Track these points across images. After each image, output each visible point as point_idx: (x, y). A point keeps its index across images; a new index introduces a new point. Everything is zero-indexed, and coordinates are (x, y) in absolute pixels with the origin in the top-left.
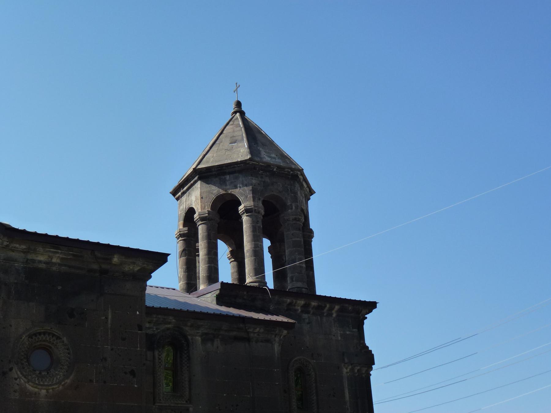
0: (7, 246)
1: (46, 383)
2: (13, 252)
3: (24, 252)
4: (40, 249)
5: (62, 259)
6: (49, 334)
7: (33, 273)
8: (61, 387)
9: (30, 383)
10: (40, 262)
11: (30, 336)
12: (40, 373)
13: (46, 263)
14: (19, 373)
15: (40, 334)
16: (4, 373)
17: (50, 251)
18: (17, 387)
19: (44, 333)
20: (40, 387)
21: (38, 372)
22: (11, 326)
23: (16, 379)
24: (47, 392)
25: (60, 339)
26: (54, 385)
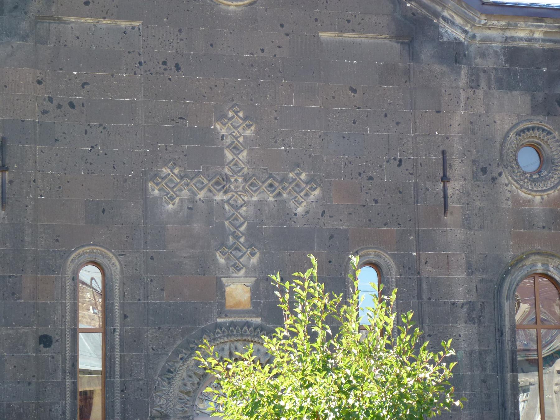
0: (485, 24)
1: (540, 189)
2: (490, 29)
3: (501, 29)
4: (522, 24)
5: (546, 33)
6: (539, 128)
7: (513, 53)
8: (556, 192)
9: (523, 189)
10: (521, 39)
11: (518, 134)
12: (531, 176)
13: (529, 40)
14: (510, 178)
15: (528, 129)
16: (494, 179)
17: (532, 25)
18: (508, 195)
19: (533, 128)
20: (534, 193)
21: (528, 175)
22: (495, 122)
23: (507, 185)
24: (542, 199)
25: (551, 134)
26: (548, 190)
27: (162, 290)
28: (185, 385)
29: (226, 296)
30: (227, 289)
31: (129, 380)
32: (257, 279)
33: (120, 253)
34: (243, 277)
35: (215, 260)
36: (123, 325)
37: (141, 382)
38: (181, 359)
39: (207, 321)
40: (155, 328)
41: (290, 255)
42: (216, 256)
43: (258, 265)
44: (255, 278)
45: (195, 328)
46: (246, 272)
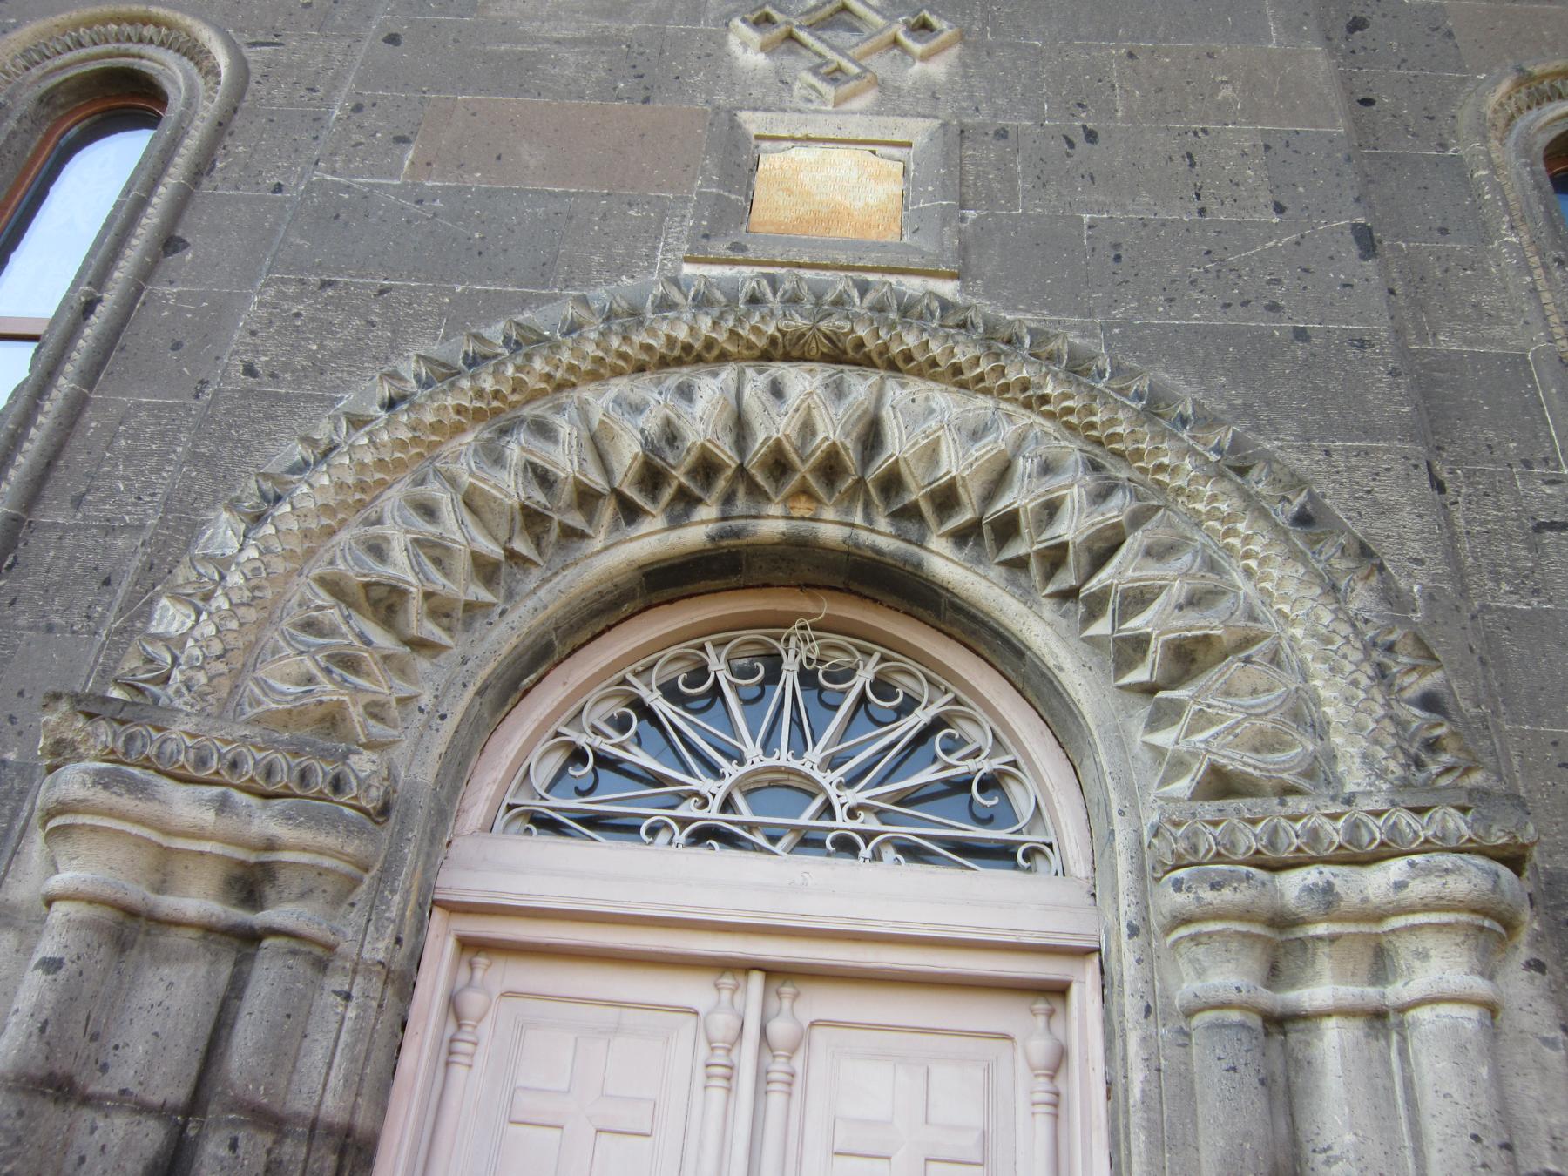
27: (402, 140)
28: (378, 550)
29: (759, 185)
30: (771, 162)
31: (55, 525)
32: (944, 125)
33: (260, 39)
34: (861, 113)
35: (715, 54)
36: (146, 274)
37: (121, 542)
38: (390, 404)
39: (624, 268)
40: (302, 282)
41: (1131, 55)
42: (722, 44)
43: (950, 81)
44: (936, 123)
45: (538, 297)
46: (881, 102)
